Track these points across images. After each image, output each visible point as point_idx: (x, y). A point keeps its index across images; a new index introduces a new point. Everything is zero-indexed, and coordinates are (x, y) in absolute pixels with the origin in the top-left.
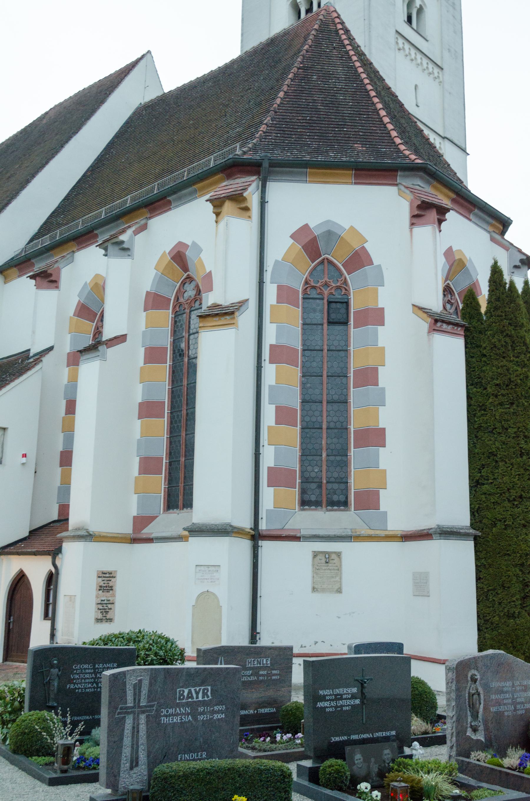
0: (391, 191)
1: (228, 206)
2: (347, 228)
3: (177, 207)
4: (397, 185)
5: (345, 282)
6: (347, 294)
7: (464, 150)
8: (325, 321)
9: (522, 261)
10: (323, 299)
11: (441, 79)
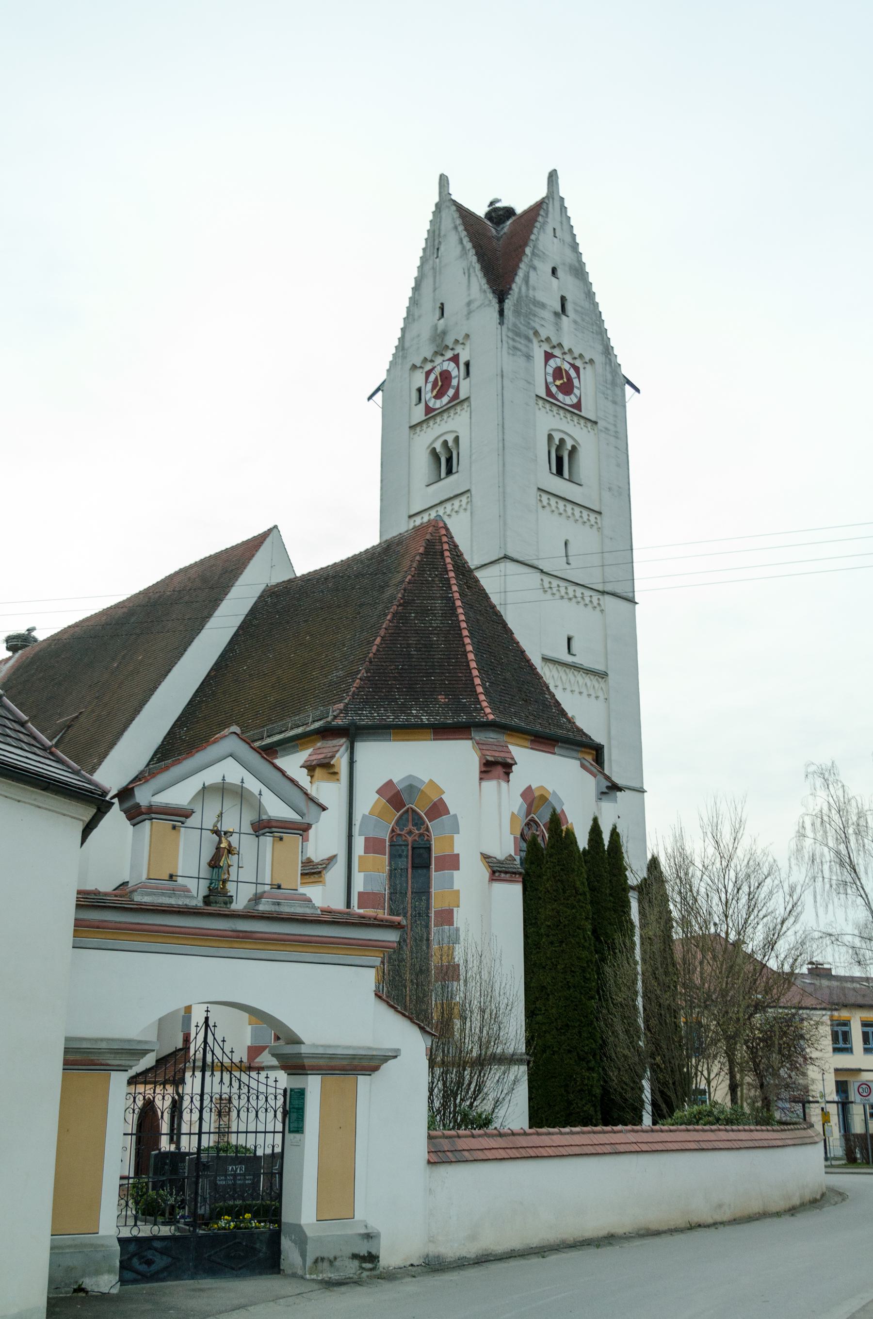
0: (469, 743)
1: (318, 772)
2: (427, 781)
3: (283, 756)
4: (471, 739)
5: (427, 830)
6: (429, 841)
7: (632, 601)
8: (410, 865)
9: (608, 787)
10: (407, 845)
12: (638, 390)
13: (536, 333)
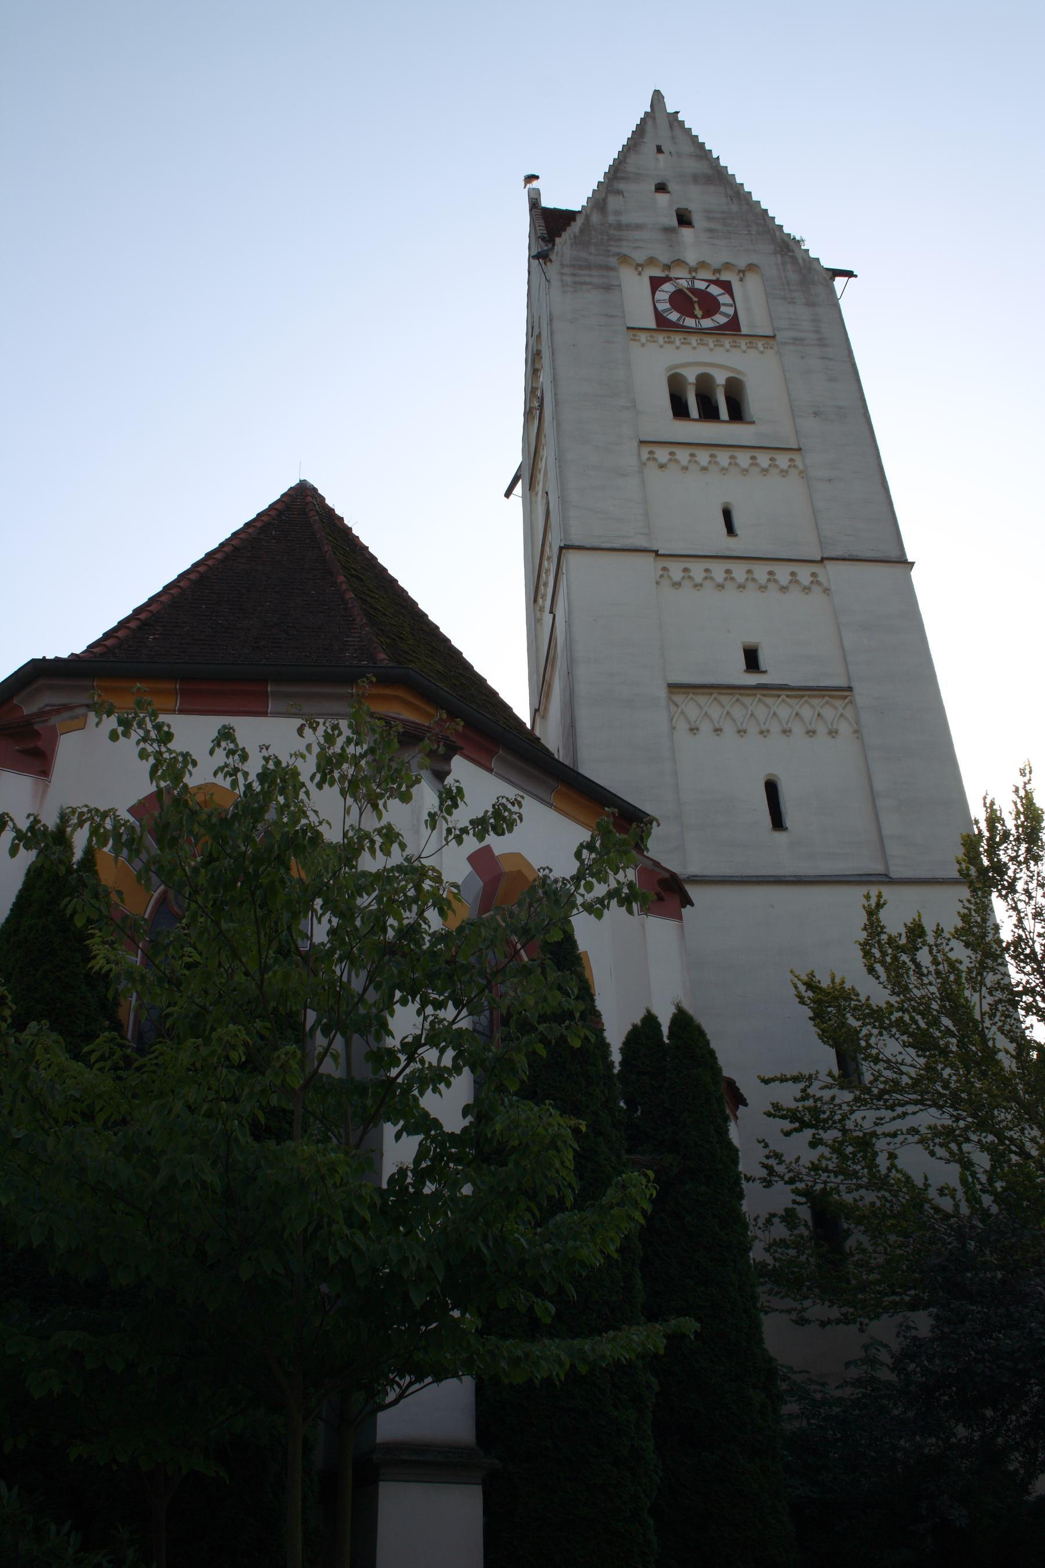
11: (801, 467)
12: (849, 274)
13: (624, 259)
